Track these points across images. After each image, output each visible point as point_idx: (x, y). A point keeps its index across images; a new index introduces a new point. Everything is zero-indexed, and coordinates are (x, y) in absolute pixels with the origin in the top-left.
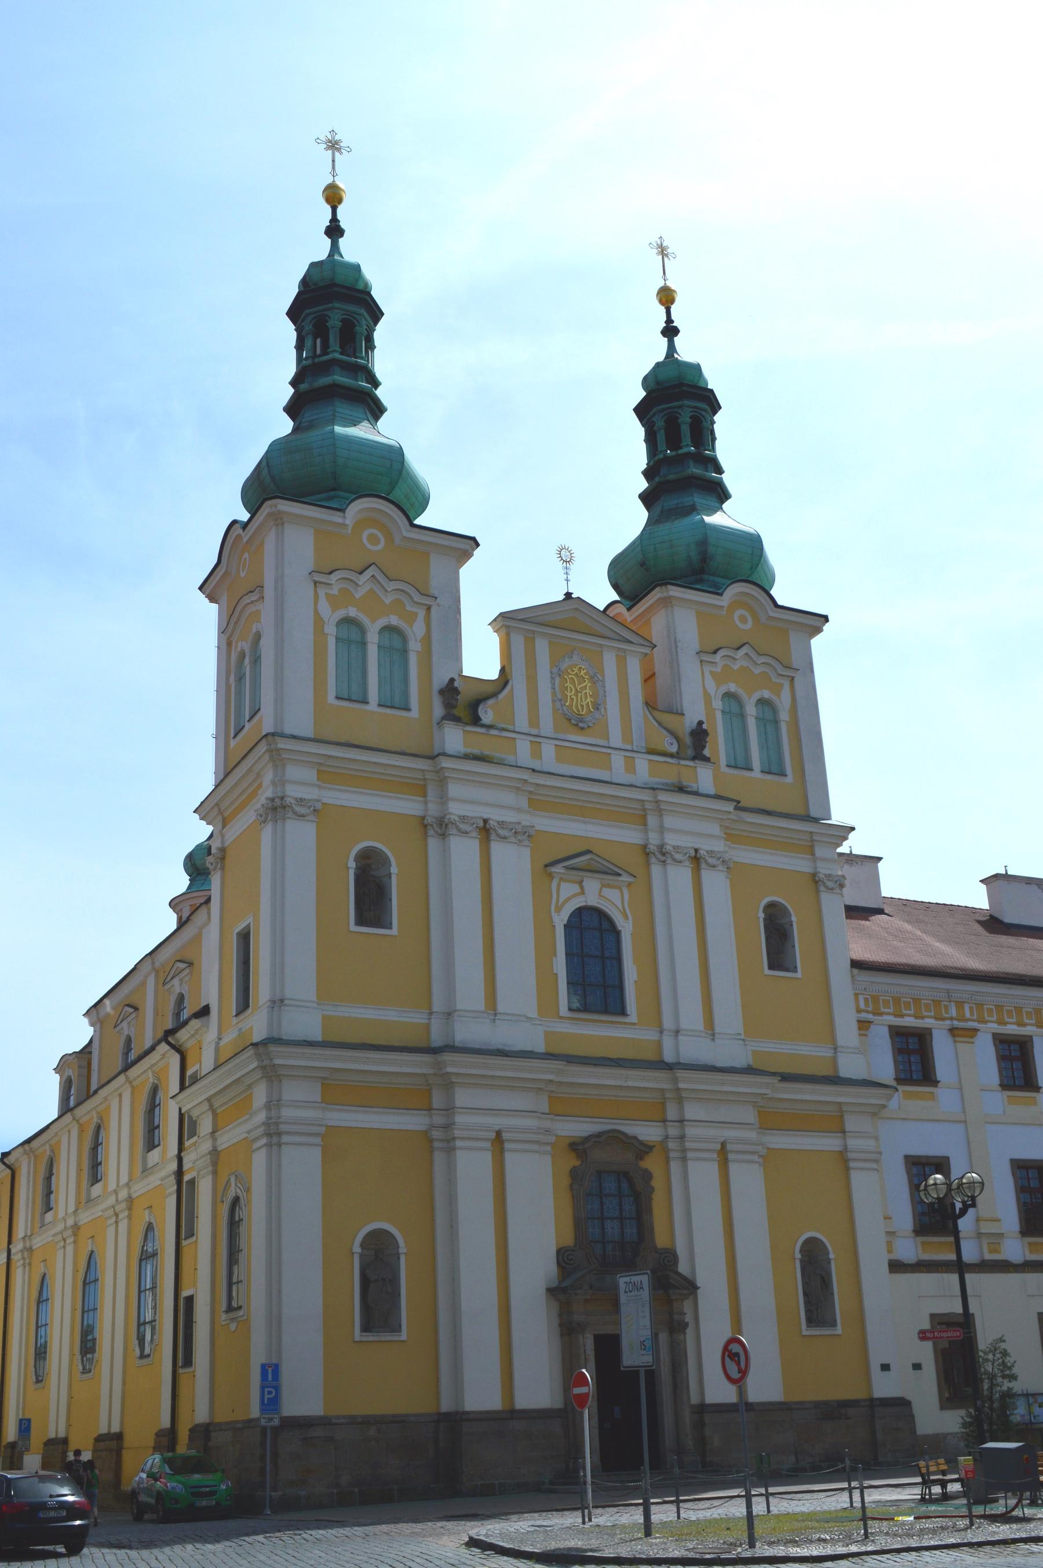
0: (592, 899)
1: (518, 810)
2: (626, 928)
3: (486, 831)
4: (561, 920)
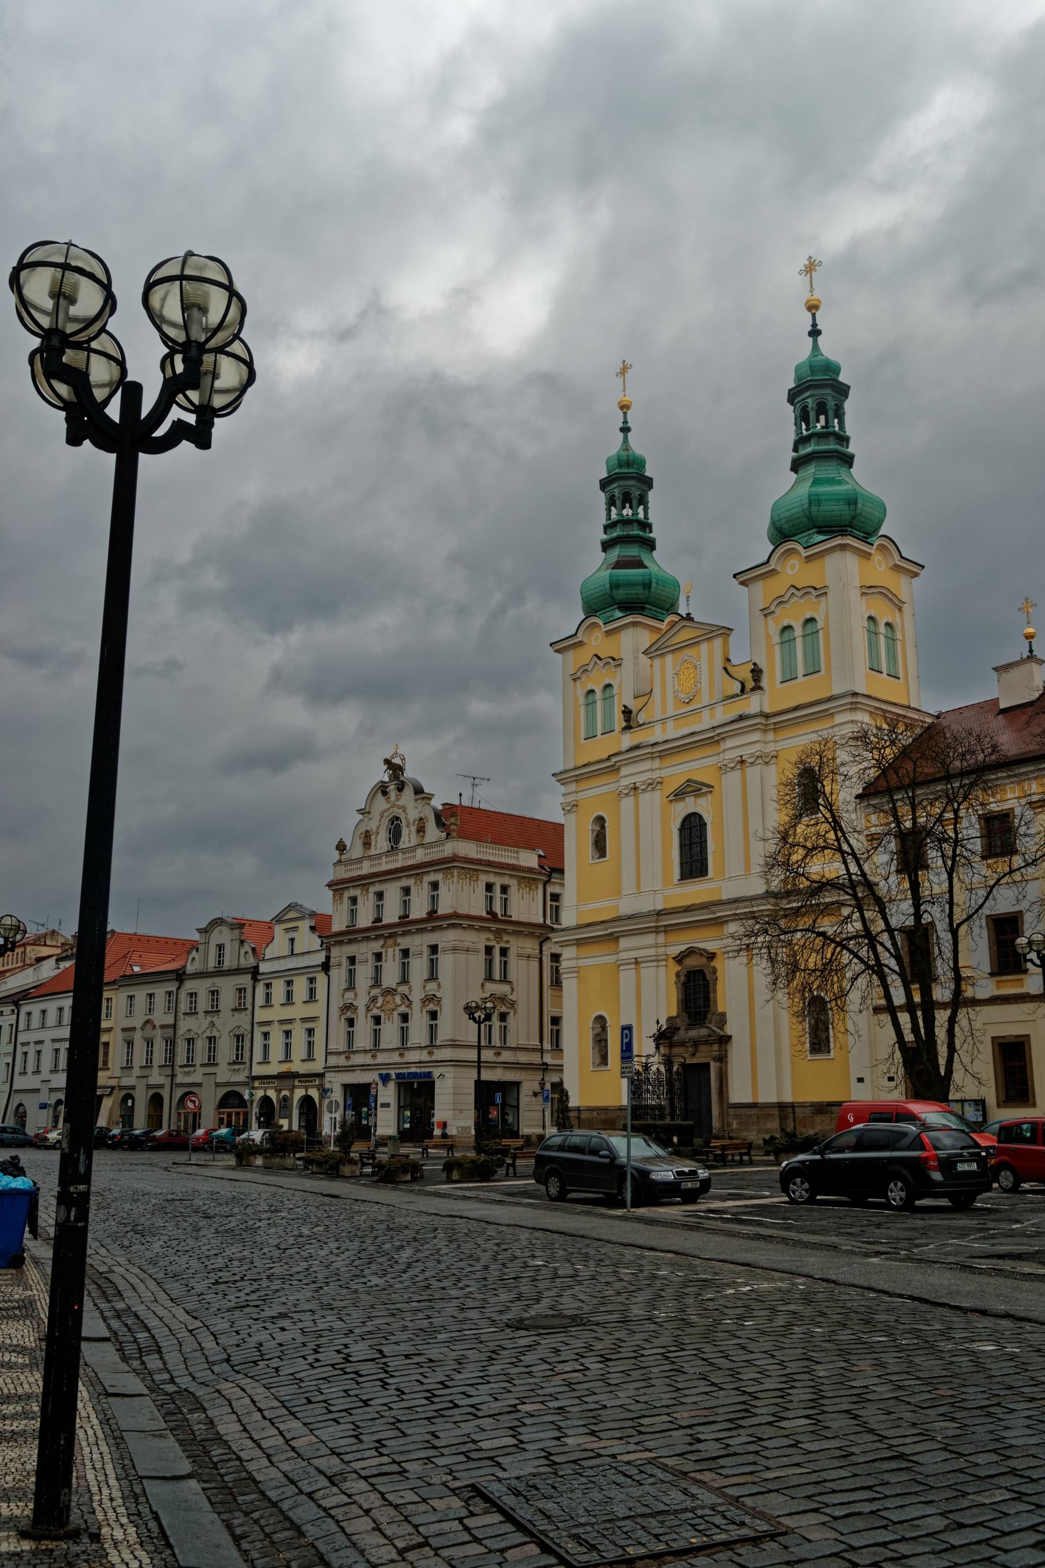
1: (652, 770)
2: (708, 818)
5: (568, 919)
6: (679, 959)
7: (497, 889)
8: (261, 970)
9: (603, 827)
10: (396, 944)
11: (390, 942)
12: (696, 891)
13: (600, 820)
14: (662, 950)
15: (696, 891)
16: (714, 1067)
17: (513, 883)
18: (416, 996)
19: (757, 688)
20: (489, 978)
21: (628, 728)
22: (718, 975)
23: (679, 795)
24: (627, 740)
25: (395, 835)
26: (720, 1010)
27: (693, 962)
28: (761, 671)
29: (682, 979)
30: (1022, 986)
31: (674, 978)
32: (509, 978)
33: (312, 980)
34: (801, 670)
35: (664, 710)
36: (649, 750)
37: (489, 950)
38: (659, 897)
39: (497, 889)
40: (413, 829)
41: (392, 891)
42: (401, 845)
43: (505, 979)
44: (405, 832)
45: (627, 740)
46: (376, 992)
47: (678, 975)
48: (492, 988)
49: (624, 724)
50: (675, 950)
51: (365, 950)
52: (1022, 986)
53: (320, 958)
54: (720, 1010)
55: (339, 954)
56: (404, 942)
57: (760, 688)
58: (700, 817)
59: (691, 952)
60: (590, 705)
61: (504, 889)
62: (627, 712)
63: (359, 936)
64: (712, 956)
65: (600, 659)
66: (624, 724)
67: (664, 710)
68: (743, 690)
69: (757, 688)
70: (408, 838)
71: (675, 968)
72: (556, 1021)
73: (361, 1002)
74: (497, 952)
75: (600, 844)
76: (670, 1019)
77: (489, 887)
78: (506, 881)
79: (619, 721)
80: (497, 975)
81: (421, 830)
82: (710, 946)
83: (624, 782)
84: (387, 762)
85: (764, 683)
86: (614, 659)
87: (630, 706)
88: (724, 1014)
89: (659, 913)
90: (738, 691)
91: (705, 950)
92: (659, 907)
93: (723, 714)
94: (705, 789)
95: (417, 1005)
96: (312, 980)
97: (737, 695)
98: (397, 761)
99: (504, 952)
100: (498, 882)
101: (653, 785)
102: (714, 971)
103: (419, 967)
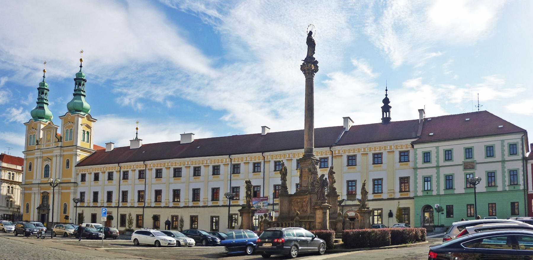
2: (50, 166)
3: (37, 158)
4: (44, 167)
6: (43, 193)
9: (31, 164)
12: (45, 180)
13: (31, 163)
14: (39, 191)
16: (47, 214)
21: (37, 145)
22: (49, 197)
28: (62, 138)
30: (198, 204)
31: (41, 197)
35: (44, 143)
36: (40, 150)
37: (8, 187)
38: (40, 181)
43: (12, 193)
45: (36, 147)
47: (42, 196)
49: (37, 144)
50: (42, 191)
52: (198, 204)
58: (49, 166)
59: (44, 192)
60: (30, 138)
61: (13, 174)
62: (37, 141)
65: (33, 129)
66: (37, 144)
67: (44, 143)
68: (58, 141)
69: (61, 141)
71: (42, 195)
75: (30, 167)
76: (40, 205)
77: (9, 173)
78: (14, 172)
79: (36, 143)
83: (36, 156)
85: (62, 140)
86: (36, 129)
89: (39, 184)
90: (57, 141)
91: (47, 192)
92: (40, 183)
94: (50, 160)
97: (57, 142)
100: (12, 173)
101: (40, 157)
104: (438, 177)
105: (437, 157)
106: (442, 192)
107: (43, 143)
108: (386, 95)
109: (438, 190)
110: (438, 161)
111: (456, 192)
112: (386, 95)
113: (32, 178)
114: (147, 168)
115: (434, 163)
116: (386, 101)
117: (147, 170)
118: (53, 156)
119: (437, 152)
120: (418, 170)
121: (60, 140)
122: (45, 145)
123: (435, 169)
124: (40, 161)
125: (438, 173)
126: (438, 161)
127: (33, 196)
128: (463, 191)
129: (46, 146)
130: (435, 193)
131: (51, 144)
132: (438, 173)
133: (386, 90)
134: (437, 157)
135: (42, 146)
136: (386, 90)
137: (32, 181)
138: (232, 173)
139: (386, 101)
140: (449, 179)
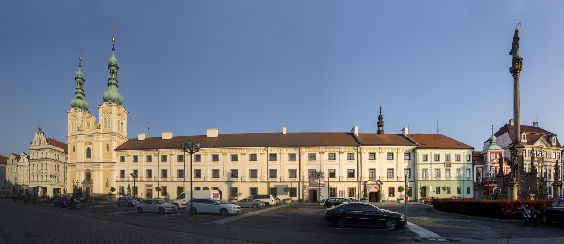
0: (89, 147)
2: (91, 149)
4: (86, 149)
5: (68, 162)
6: (85, 171)
7: (57, 155)
8: (19, 165)
10: (40, 163)
11: (39, 162)
12: (89, 160)
15: (89, 160)
17: (60, 154)
18: (44, 172)
19: (100, 128)
20: (56, 170)
21: (78, 131)
23: (87, 144)
24: (78, 133)
25: (40, 142)
26: (92, 179)
27: (88, 171)
29: (86, 174)
32: (59, 171)
33: (27, 168)
34: (107, 127)
35: (85, 129)
37: (56, 165)
39: (57, 155)
40: (43, 142)
41: (40, 152)
42: (41, 144)
43: (58, 171)
44: (42, 142)
45: (78, 133)
46: (37, 171)
47: (86, 173)
48: (56, 172)
51: (36, 163)
53: (28, 164)
54: (92, 179)
55: (31, 163)
56: (42, 162)
57: (100, 129)
61: (58, 155)
62: (78, 128)
63: (34, 160)
64: (91, 171)
67: (85, 129)
70: (42, 143)
72: (67, 179)
73: (35, 172)
74: (57, 166)
76: (84, 180)
77: (56, 154)
78: (58, 153)
79: (77, 129)
80: (57, 170)
81: (44, 142)
82: (91, 169)
83: (78, 140)
84: (39, 128)
85: (101, 127)
87: (79, 127)
88: (92, 180)
93: (94, 132)
95: (44, 174)
96: (27, 168)
98: (40, 128)
99: (58, 166)
100: (58, 153)
102: (91, 173)
103: (44, 167)
104: (431, 170)
105: (431, 158)
106: (434, 179)
107: (84, 129)
108: (380, 113)
109: (431, 177)
110: (431, 161)
111: (441, 179)
112: (380, 113)
113: (76, 159)
114: (185, 154)
115: (429, 162)
116: (380, 118)
117: (185, 155)
118: (94, 141)
119: (431, 155)
120: (420, 165)
121: (99, 128)
122: (86, 132)
123: (430, 165)
124: (83, 144)
125: (431, 168)
126: (431, 161)
127: (78, 172)
128: (445, 179)
129: (87, 132)
130: (429, 179)
131: (91, 131)
132: (431, 168)
133: (381, 109)
134: (431, 158)
135: (83, 131)
136: (381, 109)
137: (76, 161)
138: (269, 160)
139: (380, 118)
140: (438, 171)
